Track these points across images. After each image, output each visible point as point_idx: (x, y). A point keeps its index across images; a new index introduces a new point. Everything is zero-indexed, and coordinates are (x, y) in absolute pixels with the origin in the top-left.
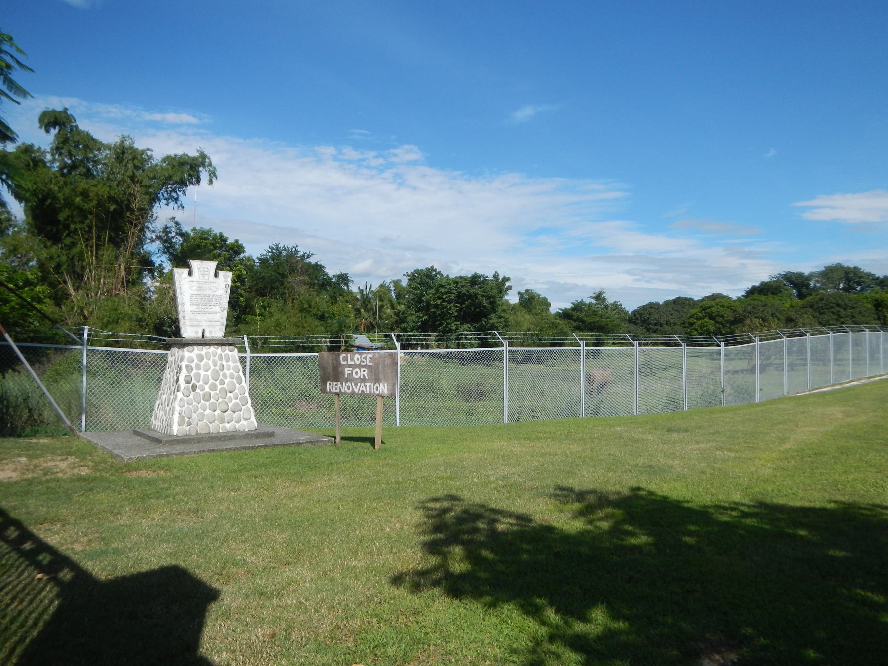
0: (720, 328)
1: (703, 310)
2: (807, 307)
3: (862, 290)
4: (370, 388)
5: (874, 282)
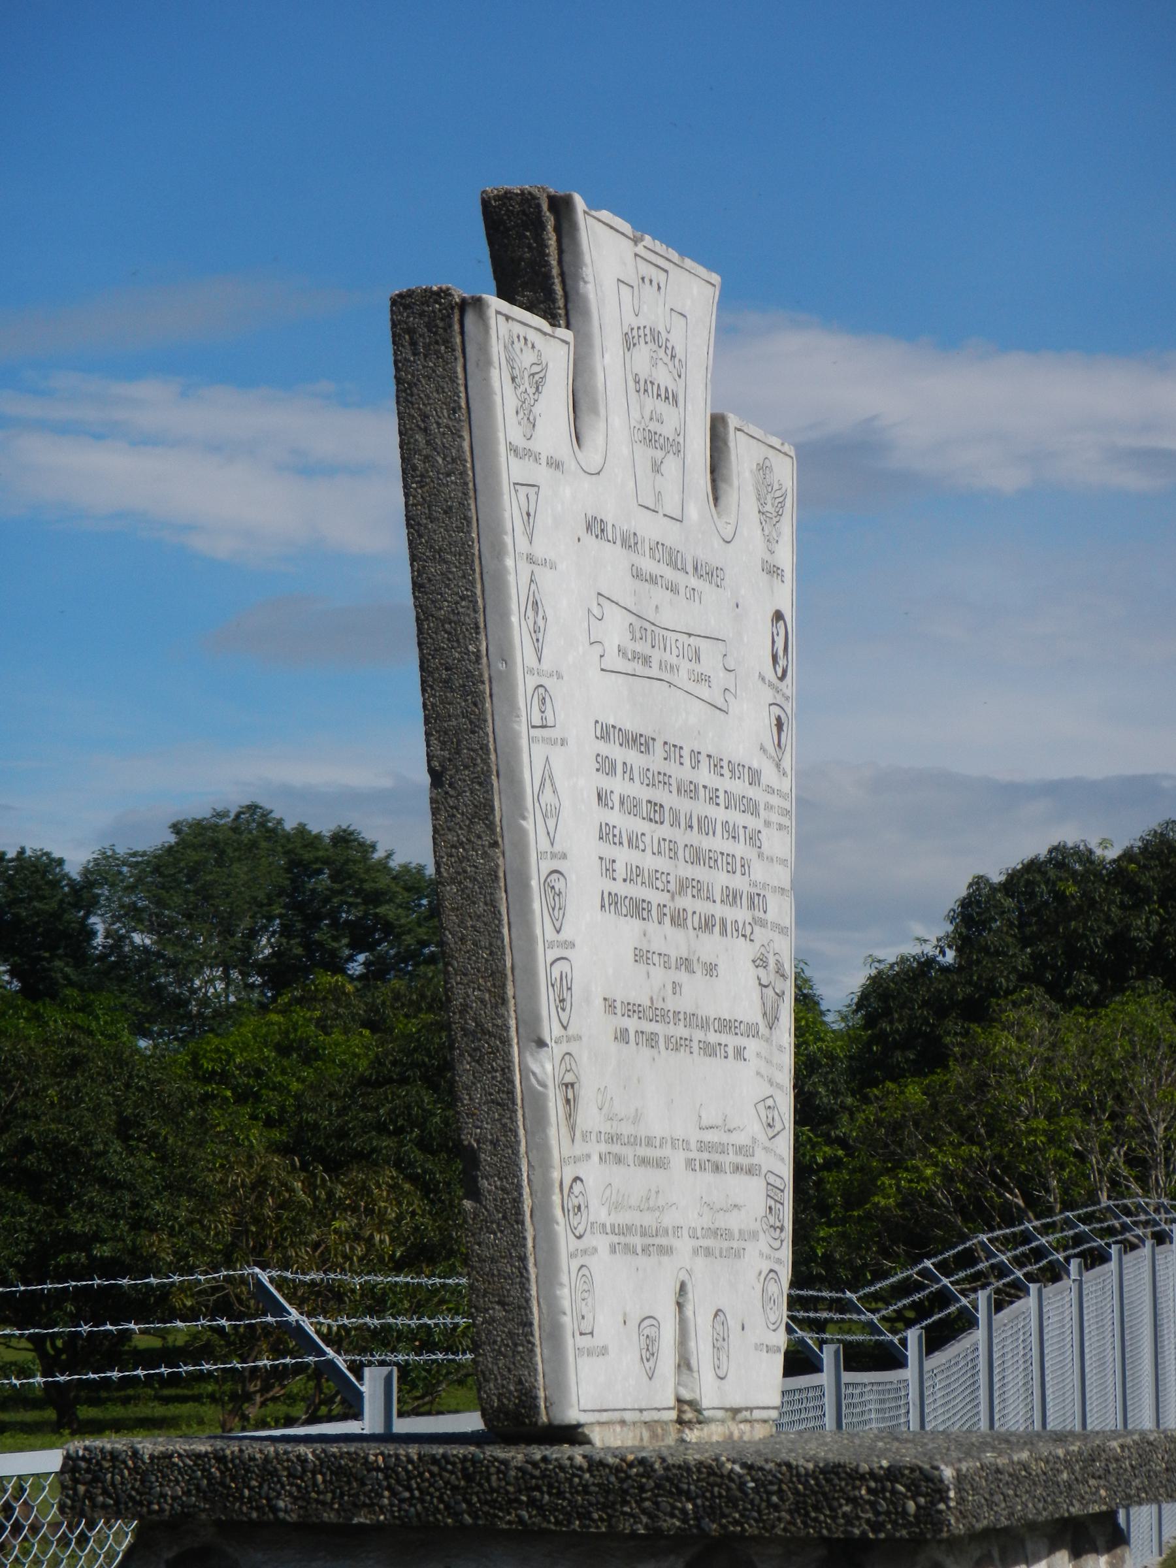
2: (403, 1081)
3: (376, 972)
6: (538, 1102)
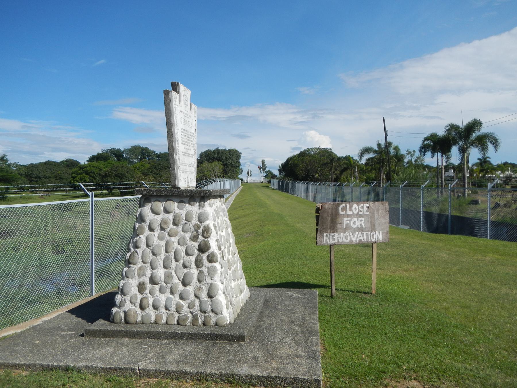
0: (92, 180)
1: (81, 169)
3: (149, 159)
4: (367, 235)
5: (155, 155)
6: (177, 160)
